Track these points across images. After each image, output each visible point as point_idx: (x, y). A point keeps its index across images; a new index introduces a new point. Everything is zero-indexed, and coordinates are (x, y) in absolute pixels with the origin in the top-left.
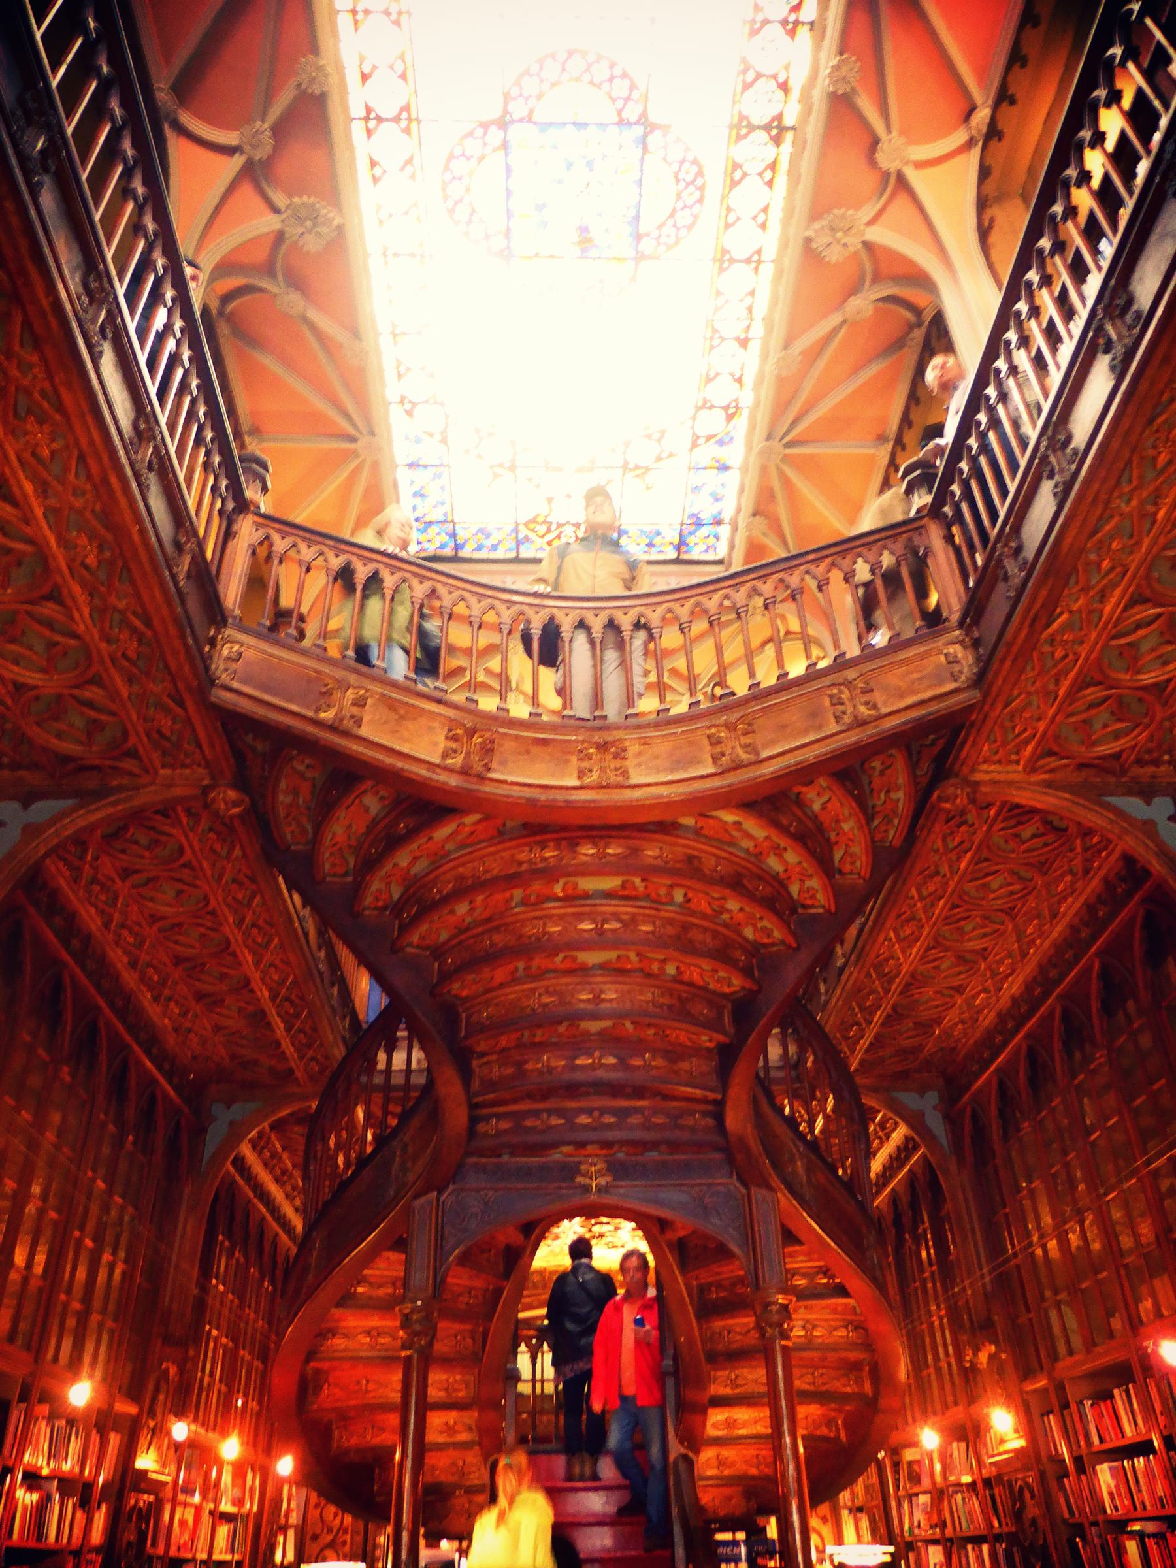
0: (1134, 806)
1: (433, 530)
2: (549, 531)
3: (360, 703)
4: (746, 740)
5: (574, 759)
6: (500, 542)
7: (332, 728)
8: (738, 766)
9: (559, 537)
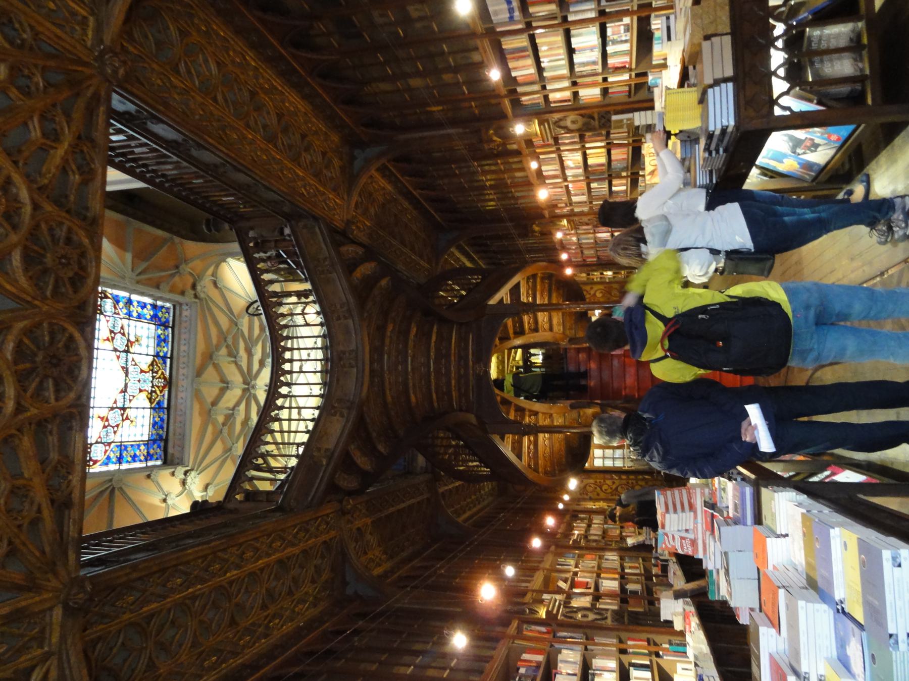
0: (357, 164)
1: (152, 451)
2: (155, 392)
3: (319, 450)
4: (338, 307)
5: (345, 369)
6: (159, 417)
7: (330, 459)
8: (349, 311)
9: (158, 387)
